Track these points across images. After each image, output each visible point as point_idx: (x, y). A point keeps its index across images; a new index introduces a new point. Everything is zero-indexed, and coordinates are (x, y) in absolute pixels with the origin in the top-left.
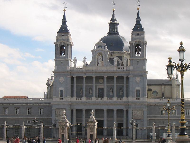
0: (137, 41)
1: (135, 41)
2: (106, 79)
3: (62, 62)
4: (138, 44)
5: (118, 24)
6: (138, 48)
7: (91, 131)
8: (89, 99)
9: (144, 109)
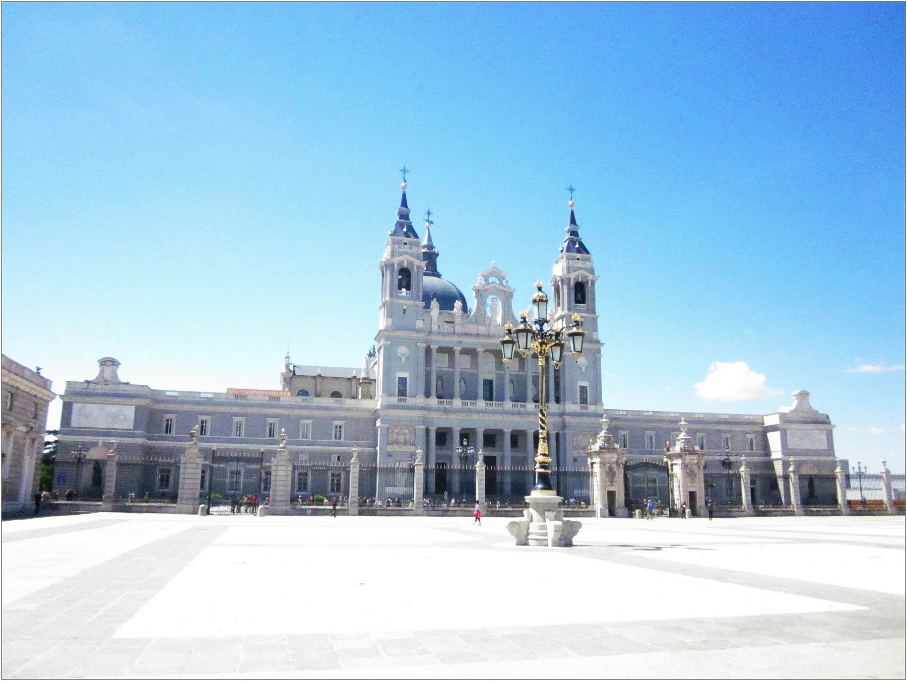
3: (405, 307)
4: (580, 281)
5: (437, 255)
7: (693, 482)
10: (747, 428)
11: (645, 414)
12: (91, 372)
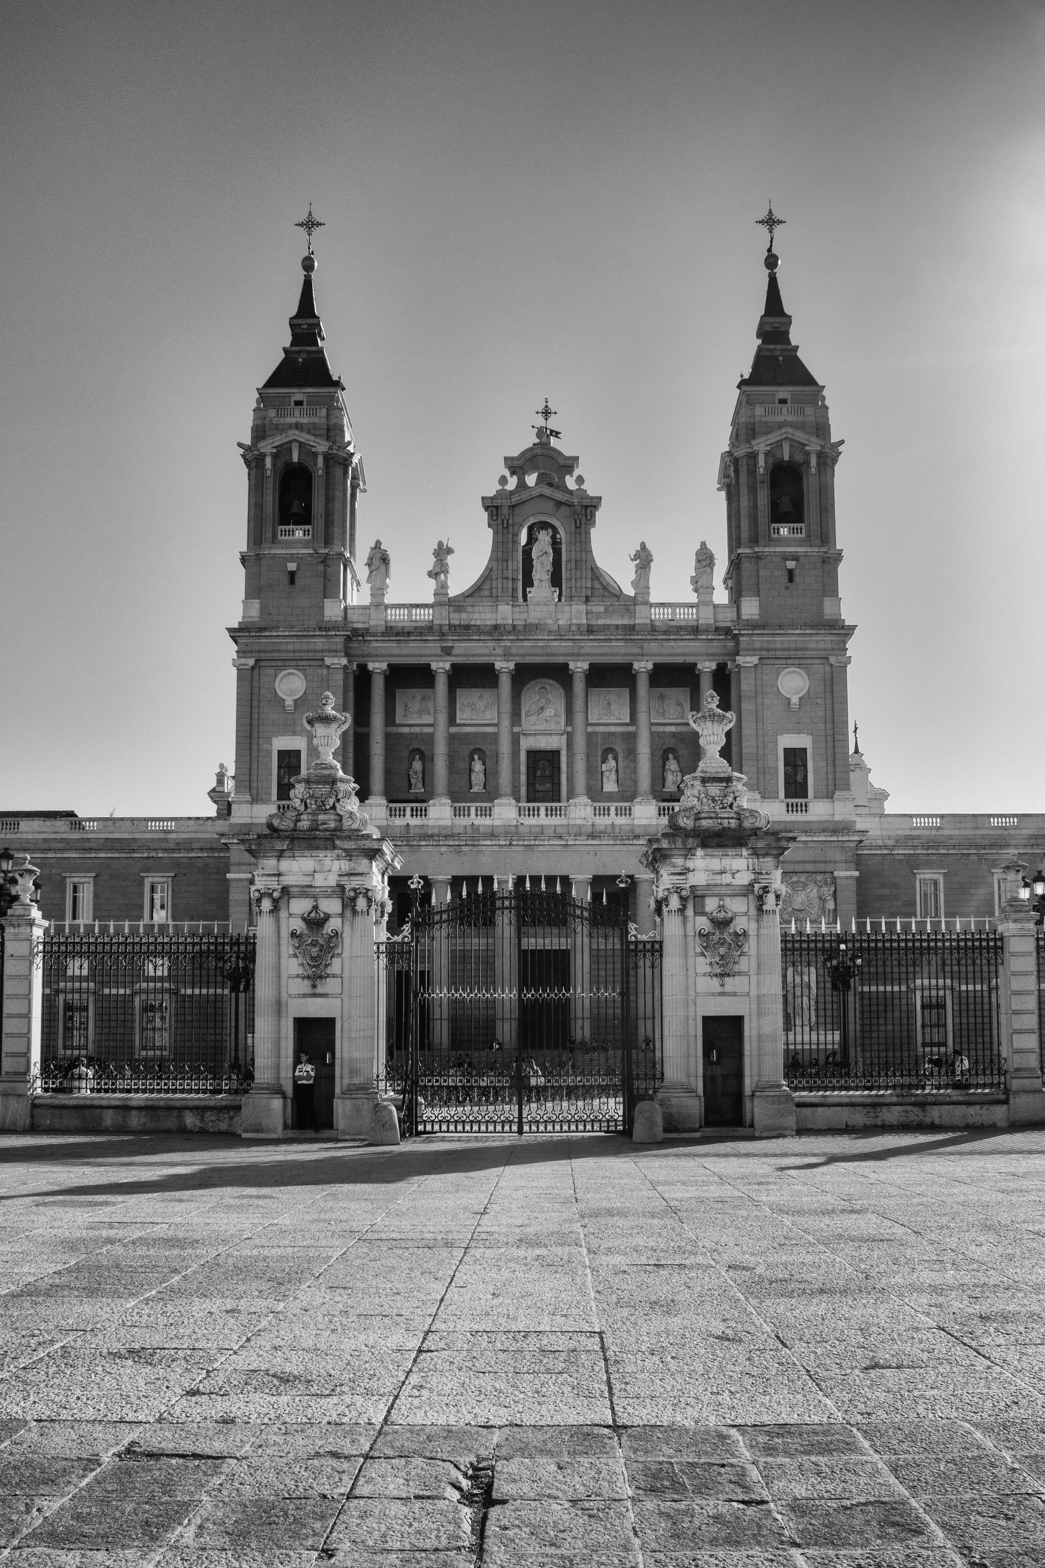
0: (779, 444)
1: (774, 438)
2: (579, 685)
3: (292, 566)
8: (473, 810)
9: (836, 874)
11: (994, 822)
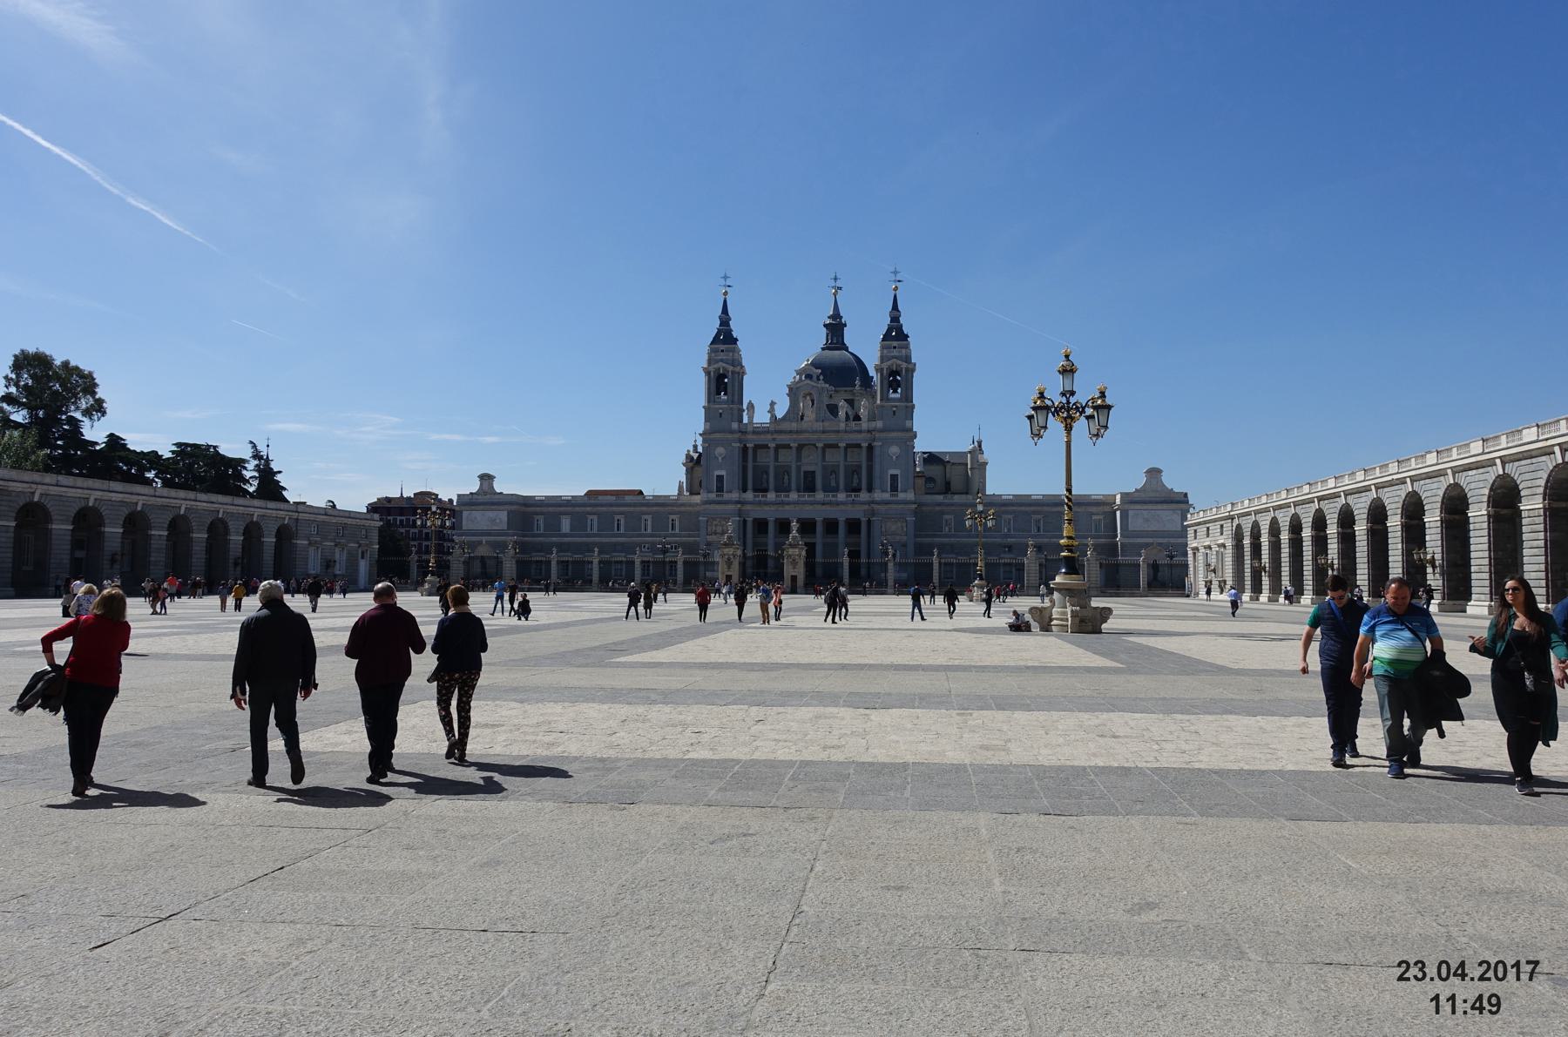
0: (892, 365)
3: (721, 411)
6: (895, 379)
10: (1093, 509)
12: (474, 486)
